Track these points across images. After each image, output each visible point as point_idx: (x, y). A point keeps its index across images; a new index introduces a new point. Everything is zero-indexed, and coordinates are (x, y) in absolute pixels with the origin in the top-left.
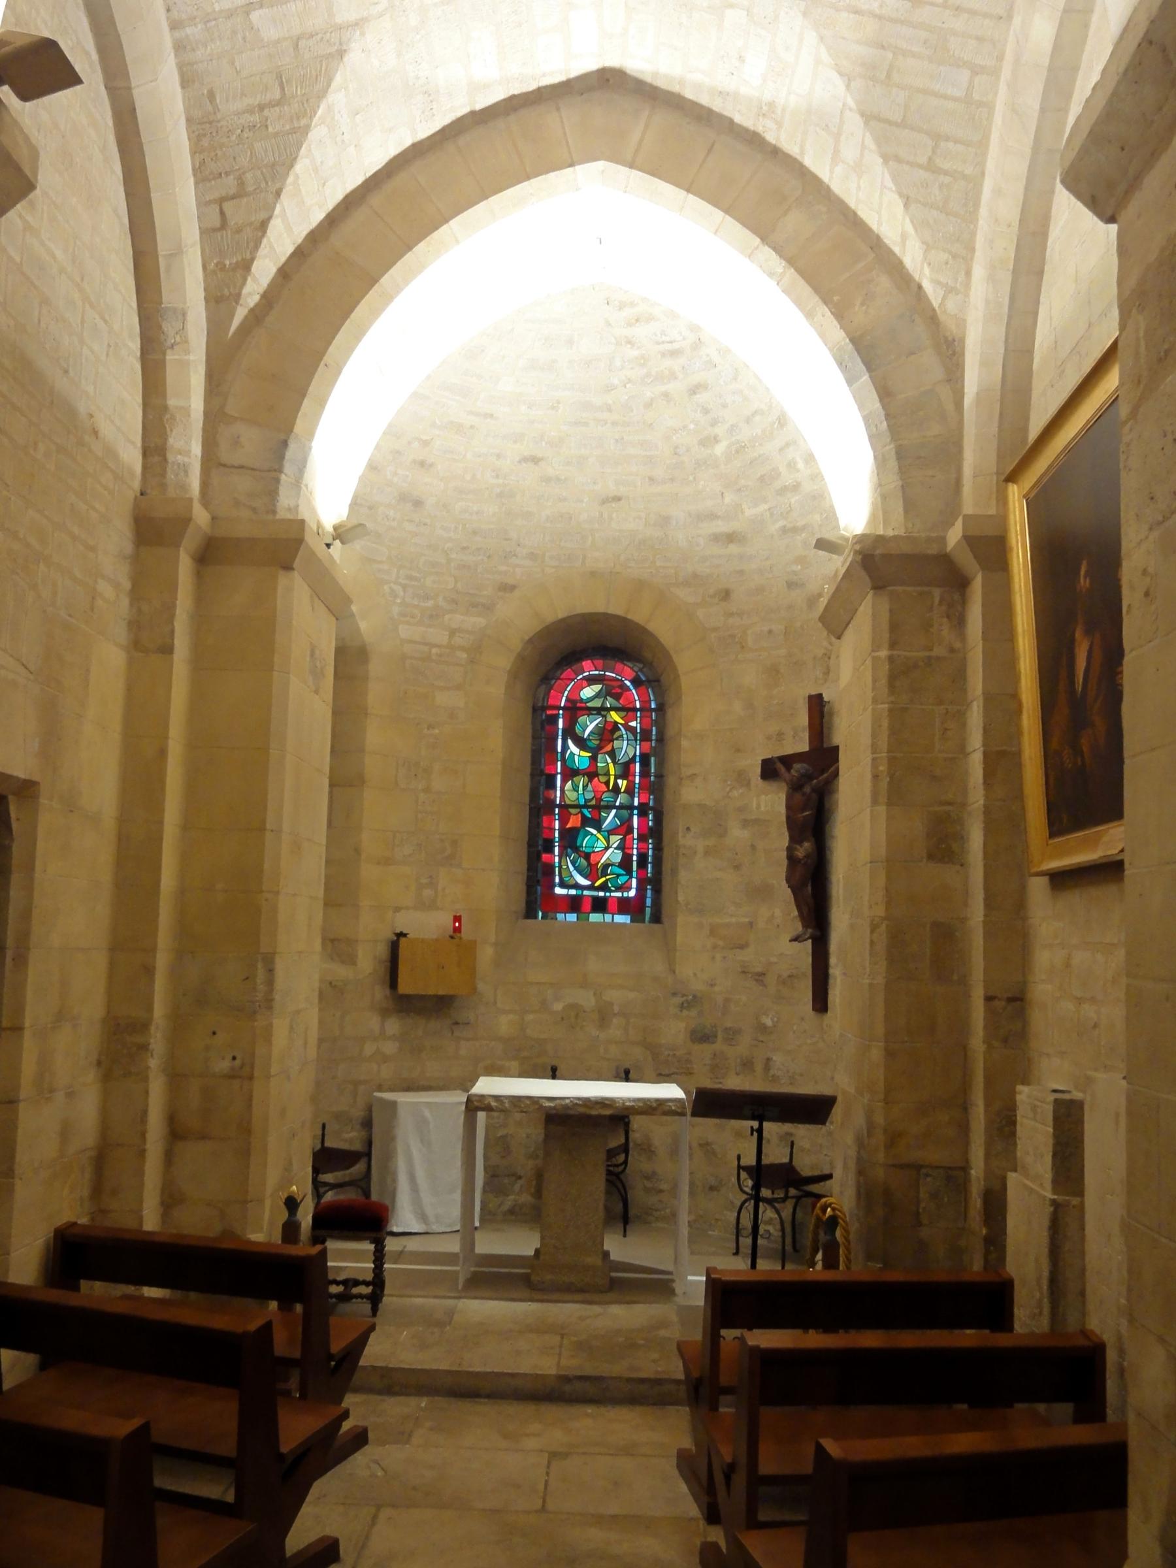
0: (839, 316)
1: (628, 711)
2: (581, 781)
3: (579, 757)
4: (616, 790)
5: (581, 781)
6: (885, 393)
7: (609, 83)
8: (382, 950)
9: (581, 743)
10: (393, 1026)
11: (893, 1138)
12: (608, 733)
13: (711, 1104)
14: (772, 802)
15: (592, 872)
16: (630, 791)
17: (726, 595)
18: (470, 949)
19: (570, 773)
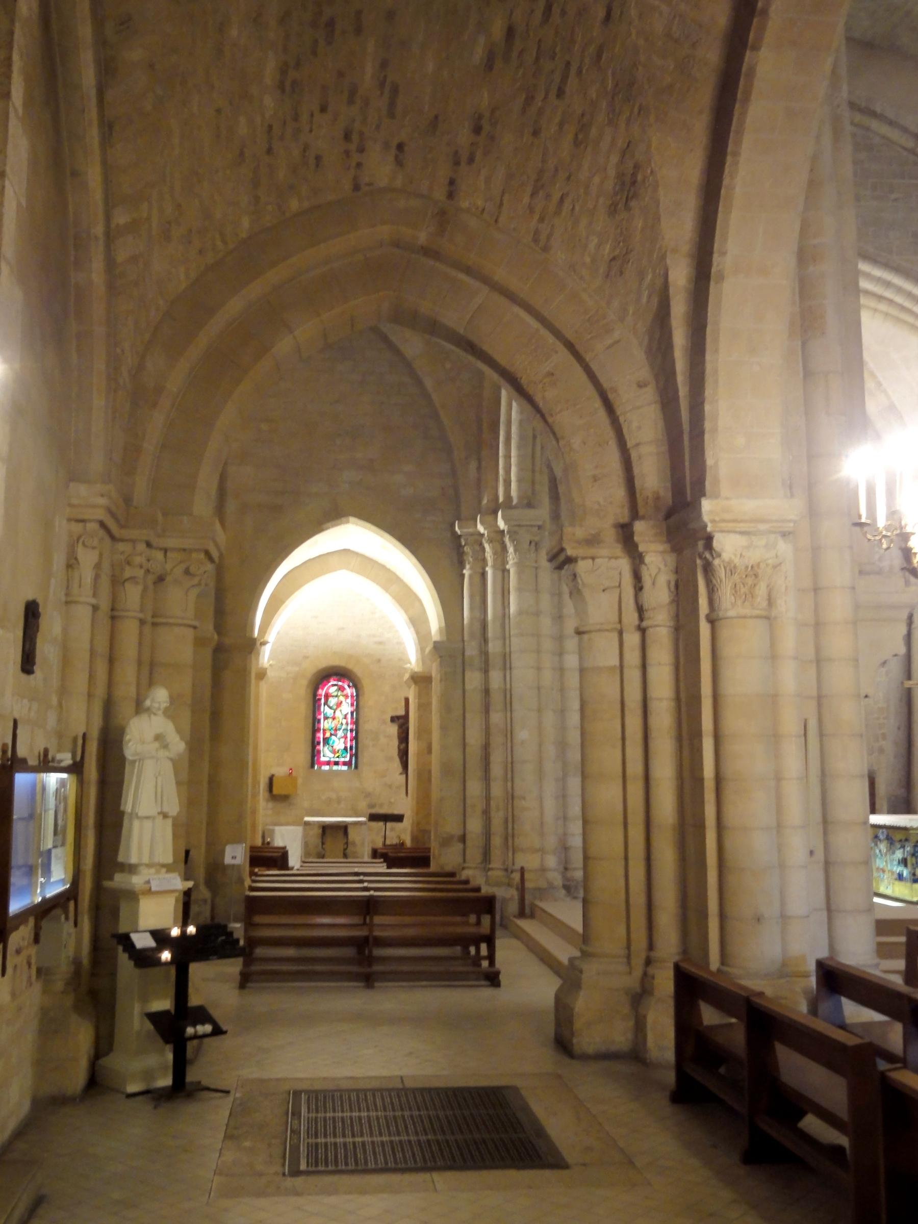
0: (406, 612)
1: (346, 696)
2: (330, 720)
3: (329, 712)
4: (342, 724)
5: (330, 720)
6: (417, 633)
7: (346, 551)
8: (267, 780)
9: (331, 708)
10: (270, 805)
11: (418, 824)
12: (339, 704)
13: (374, 818)
14: (394, 730)
15: (334, 752)
16: (347, 724)
17: (379, 661)
18: (295, 779)
19: (326, 718)
